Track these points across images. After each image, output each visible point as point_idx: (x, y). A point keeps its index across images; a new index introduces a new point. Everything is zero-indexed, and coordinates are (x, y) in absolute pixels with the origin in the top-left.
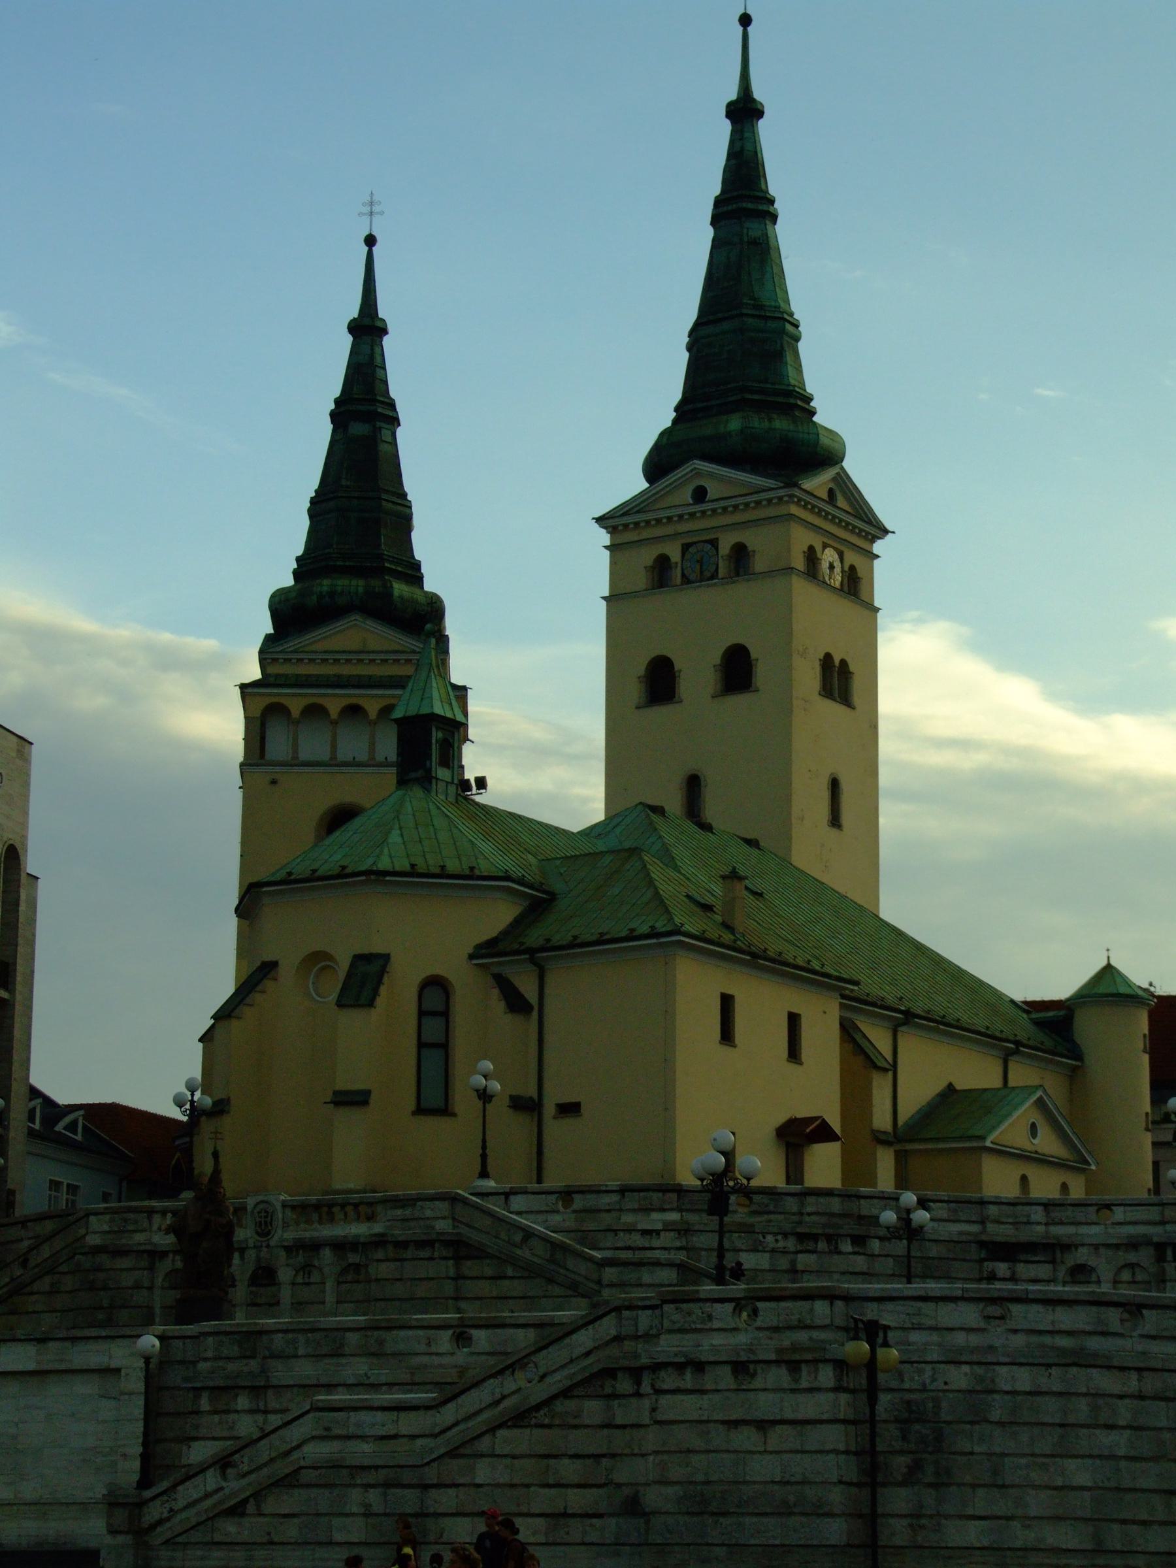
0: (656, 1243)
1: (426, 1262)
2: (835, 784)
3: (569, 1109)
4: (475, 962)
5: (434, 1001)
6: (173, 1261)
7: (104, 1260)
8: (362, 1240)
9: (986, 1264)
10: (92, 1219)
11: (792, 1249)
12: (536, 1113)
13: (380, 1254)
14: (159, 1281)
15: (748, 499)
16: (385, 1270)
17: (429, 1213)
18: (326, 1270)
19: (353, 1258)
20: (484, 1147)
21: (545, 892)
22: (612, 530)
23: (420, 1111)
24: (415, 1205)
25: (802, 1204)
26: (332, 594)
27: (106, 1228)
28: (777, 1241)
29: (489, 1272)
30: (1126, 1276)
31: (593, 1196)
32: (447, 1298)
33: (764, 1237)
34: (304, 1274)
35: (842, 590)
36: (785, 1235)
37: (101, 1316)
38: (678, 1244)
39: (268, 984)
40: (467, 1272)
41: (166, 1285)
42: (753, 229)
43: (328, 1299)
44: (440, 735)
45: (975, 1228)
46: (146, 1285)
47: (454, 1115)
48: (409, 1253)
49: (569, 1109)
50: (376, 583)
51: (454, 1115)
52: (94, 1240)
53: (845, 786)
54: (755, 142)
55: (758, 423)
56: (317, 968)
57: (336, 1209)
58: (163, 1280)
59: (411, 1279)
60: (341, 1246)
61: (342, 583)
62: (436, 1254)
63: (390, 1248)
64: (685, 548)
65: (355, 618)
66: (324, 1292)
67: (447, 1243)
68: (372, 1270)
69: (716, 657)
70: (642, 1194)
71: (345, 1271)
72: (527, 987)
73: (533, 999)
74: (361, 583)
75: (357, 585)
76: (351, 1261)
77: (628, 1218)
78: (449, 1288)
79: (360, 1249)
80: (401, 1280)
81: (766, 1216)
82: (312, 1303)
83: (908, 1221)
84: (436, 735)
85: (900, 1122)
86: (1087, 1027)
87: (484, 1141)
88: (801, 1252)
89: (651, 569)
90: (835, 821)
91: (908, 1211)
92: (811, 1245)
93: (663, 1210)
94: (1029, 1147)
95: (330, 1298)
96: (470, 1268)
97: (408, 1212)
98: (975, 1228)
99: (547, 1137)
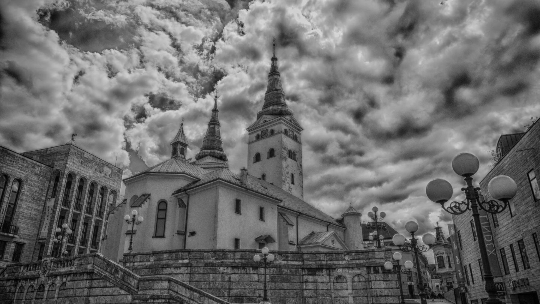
0: (179, 271)
2: (292, 176)
3: (193, 234)
4: (174, 195)
5: (162, 206)
9: (304, 276)
11: (230, 273)
15: (273, 120)
21: (198, 179)
22: (249, 131)
23: (156, 236)
25: (234, 255)
26: (204, 153)
28: (224, 270)
30: (356, 279)
33: (220, 269)
35: (293, 138)
36: (227, 267)
38: (187, 272)
40: (94, 285)
42: (275, 77)
44: (181, 147)
45: (300, 263)
47: (165, 237)
49: (193, 234)
50: (213, 151)
51: (165, 237)
53: (295, 175)
54: (276, 64)
55: (275, 107)
61: (206, 151)
64: (262, 132)
65: (208, 157)
67: (88, 273)
69: (268, 151)
70: (176, 253)
72: (185, 200)
73: (186, 205)
74: (210, 151)
75: (209, 151)
77: (171, 262)
81: (221, 260)
83: (265, 260)
84: (180, 147)
85: (299, 241)
86: (347, 220)
88: (232, 274)
89: (256, 137)
90: (293, 183)
91: (265, 255)
92: (236, 271)
93: (184, 259)
94: (332, 246)
96: (95, 283)
98: (300, 263)
99: (187, 241)
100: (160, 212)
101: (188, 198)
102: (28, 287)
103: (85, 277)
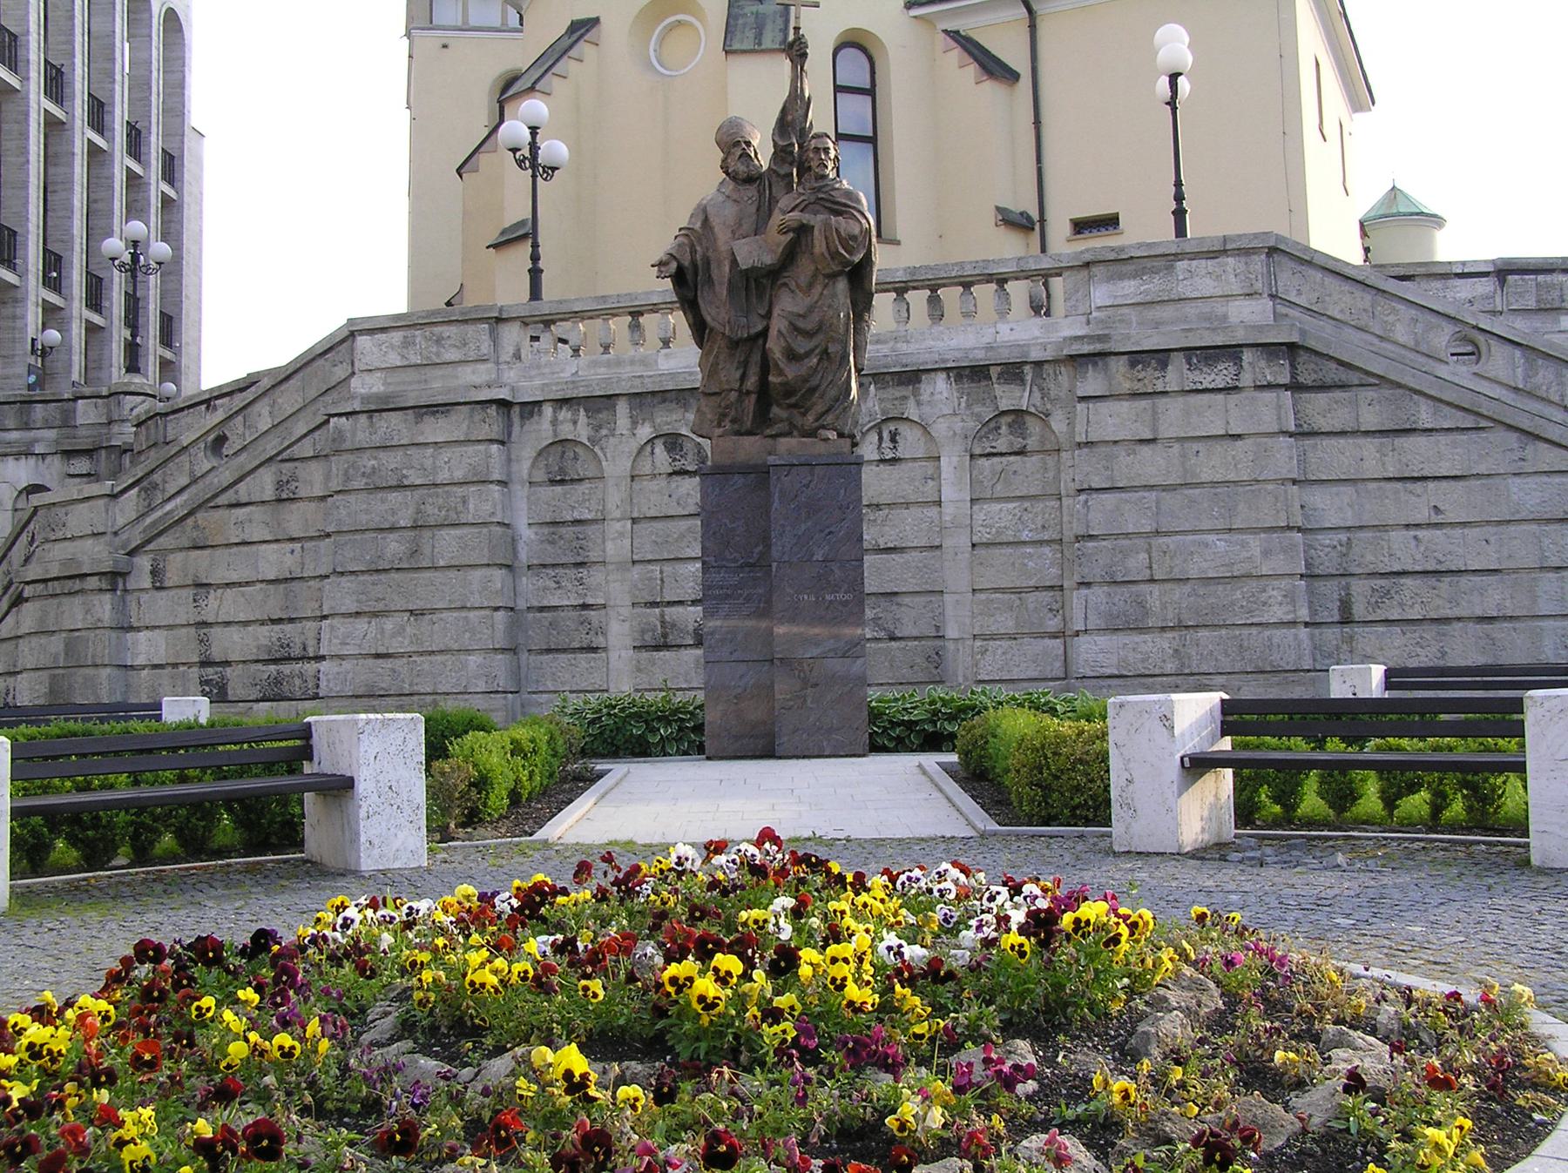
1: (1220, 397)
6: (554, 422)
7: (394, 426)
8: (1035, 355)
10: (363, 342)
12: (1036, 235)
13: (1092, 383)
14: (523, 468)
16: (1115, 420)
17: (1206, 286)
18: (940, 429)
19: (1009, 397)
20: (1179, 198)
24: (1170, 268)
27: (394, 359)
29: (1371, 418)
31: (1437, 284)
32: (1284, 481)
34: (881, 439)
37: (394, 546)
39: (583, 48)
40: (1323, 424)
41: (540, 476)
43: (948, 493)
46: (496, 477)
48: (1176, 375)
51: (898, 243)
52: (366, 386)
56: (660, 28)
57: (949, 295)
58: (533, 465)
59: (1179, 439)
60: (972, 374)
62: (1246, 379)
63: (1119, 366)
66: (936, 477)
67: (1270, 350)
68: (1058, 423)
70: (1541, 278)
71: (989, 427)
76: (1004, 405)
78: (1284, 457)
79: (1029, 378)
80: (1153, 441)
82: (907, 505)
87: (1178, 184)
95: (953, 491)
96: (1324, 410)
97: (1153, 286)
100: (848, 102)
101: (1033, 27)
102: (634, 445)
103: (1255, 368)
